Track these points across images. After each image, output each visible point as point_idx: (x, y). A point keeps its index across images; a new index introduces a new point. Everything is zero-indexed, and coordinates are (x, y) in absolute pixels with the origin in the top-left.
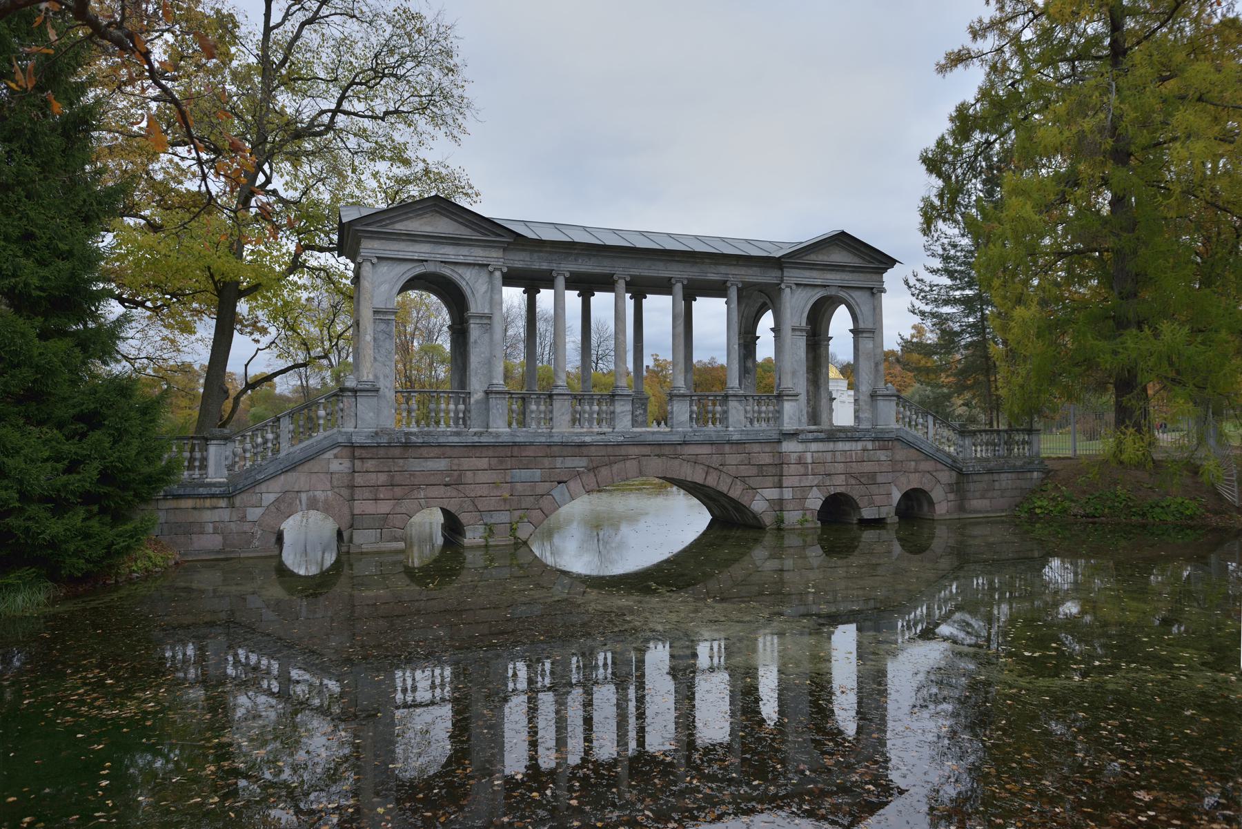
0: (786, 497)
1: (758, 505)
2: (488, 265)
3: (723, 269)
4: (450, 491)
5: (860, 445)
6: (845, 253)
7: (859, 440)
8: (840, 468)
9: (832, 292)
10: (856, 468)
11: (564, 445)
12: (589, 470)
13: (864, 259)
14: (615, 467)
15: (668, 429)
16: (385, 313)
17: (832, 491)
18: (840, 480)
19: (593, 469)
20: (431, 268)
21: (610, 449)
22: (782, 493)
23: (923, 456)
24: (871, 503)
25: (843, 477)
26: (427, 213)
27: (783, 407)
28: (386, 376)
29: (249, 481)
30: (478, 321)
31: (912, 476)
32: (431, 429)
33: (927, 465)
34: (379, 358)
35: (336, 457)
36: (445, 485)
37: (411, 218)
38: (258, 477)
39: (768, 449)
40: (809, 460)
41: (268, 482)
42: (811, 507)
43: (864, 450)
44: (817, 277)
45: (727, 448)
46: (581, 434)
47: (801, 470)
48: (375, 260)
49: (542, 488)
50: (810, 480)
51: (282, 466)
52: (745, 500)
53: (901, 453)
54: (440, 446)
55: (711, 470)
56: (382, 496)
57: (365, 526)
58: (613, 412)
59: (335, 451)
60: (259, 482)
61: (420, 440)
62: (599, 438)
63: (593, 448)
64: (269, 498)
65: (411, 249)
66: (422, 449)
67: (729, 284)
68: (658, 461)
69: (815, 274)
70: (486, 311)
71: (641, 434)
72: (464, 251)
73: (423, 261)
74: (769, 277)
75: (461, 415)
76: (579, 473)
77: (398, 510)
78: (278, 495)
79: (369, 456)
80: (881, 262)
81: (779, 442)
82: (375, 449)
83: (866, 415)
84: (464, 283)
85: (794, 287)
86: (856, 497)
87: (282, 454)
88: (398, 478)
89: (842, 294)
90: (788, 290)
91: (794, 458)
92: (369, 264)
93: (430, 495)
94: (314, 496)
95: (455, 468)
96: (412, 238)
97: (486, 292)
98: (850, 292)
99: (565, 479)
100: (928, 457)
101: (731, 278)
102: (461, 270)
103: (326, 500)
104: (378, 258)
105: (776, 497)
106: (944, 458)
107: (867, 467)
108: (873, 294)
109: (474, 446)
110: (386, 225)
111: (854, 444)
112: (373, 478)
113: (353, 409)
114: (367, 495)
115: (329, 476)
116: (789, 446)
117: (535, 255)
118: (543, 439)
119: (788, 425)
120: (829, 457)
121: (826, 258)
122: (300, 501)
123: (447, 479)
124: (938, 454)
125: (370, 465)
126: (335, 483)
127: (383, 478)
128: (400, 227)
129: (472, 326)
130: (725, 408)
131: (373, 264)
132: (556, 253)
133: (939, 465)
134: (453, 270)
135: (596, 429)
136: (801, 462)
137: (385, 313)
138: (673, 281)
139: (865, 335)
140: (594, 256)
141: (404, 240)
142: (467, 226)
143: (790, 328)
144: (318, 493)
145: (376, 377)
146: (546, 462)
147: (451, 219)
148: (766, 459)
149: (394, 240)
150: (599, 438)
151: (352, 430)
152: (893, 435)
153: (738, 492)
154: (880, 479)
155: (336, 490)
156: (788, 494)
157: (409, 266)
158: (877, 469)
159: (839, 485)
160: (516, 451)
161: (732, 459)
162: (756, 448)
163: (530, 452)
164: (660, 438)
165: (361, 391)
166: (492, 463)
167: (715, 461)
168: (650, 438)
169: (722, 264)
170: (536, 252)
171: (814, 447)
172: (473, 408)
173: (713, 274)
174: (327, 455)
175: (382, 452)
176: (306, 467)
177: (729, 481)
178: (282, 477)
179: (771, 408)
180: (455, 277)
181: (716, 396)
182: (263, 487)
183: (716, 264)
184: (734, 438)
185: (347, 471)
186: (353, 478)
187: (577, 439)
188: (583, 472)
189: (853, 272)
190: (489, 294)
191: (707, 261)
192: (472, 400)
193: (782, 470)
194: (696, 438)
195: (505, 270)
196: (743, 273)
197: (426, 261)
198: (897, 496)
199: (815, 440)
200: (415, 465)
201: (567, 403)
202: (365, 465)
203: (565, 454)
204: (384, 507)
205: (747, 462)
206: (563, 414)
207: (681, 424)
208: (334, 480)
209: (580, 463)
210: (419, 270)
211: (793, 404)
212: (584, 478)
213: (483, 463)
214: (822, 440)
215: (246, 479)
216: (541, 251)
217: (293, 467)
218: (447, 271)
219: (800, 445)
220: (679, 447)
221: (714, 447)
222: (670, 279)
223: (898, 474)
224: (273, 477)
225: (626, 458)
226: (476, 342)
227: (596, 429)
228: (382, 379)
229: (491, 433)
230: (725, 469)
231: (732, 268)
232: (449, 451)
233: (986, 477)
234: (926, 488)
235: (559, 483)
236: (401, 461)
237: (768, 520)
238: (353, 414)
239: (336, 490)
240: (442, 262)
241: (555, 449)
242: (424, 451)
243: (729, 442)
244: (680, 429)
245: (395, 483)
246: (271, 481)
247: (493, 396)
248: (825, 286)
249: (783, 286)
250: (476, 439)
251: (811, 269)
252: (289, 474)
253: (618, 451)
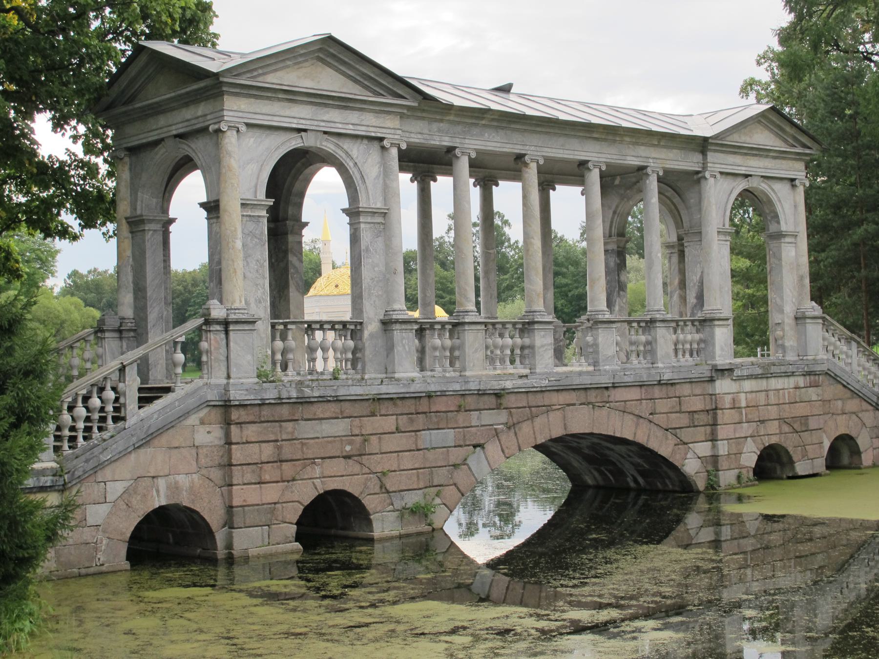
0: (721, 453)
1: (691, 467)
2: (381, 139)
3: (643, 151)
4: (353, 466)
5: (790, 382)
6: (767, 133)
7: (793, 374)
8: (773, 412)
9: (754, 183)
10: (789, 412)
11: (481, 393)
12: (509, 428)
13: (786, 141)
14: (538, 421)
15: (591, 368)
16: (254, 206)
18: (773, 427)
19: (510, 427)
20: (309, 141)
21: (530, 396)
22: (714, 447)
23: (849, 394)
24: (804, 455)
25: (776, 423)
26: (306, 61)
27: (712, 336)
28: (259, 301)
29: (92, 464)
30: (369, 219)
31: (842, 419)
32: (499, 372)
33: (853, 404)
34: (248, 274)
35: (202, 423)
36: (345, 457)
37: (288, 67)
38: (103, 458)
39: (698, 391)
40: (743, 404)
41: (114, 465)
42: (747, 464)
45: (657, 392)
46: (499, 377)
48: (243, 128)
49: (456, 455)
50: (746, 429)
51: (134, 439)
52: (676, 460)
53: (830, 390)
54: (337, 400)
55: (641, 420)
56: (267, 477)
57: (248, 523)
58: (531, 347)
59: (203, 413)
60: (100, 466)
61: (316, 394)
62: (520, 382)
63: (512, 398)
64: (116, 489)
65: (288, 112)
66: (315, 406)
67: (649, 170)
69: (738, 159)
70: (379, 205)
71: (568, 375)
72: (353, 117)
73: (299, 130)
74: (688, 162)
75: (279, 357)
76: (497, 433)
77: (288, 496)
78: (126, 484)
79: (251, 418)
80: (804, 146)
81: (712, 380)
82: (257, 409)
83: (791, 343)
84: (351, 164)
85: (718, 175)
86: (790, 449)
87: (131, 421)
88: (288, 451)
89: (764, 186)
90: (712, 180)
91: (728, 400)
92: (235, 133)
93: (327, 473)
94: (176, 483)
95: (357, 432)
96: (290, 96)
97: (377, 177)
98: (770, 182)
99: (482, 442)
100: (855, 394)
101: (651, 163)
102: (347, 144)
103: (191, 488)
104: (248, 125)
105: (708, 453)
106: (869, 394)
107: (800, 410)
108: (794, 186)
109: (378, 400)
110: (260, 75)
111: (786, 380)
112: (254, 452)
113: (223, 350)
114: (249, 477)
115: (194, 451)
116: (723, 386)
117: (435, 126)
118: (457, 387)
121: (748, 140)
122: (158, 491)
123: (348, 448)
124: (864, 391)
125: (251, 432)
126: (203, 461)
127: (268, 451)
128: (273, 79)
129: (362, 226)
130: (650, 338)
131: (238, 131)
132: (459, 123)
133: (864, 404)
134: (337, 145)
135: (510, 370)
137: (254, 206)
138: (590, 165)
139: (787, 240)
140: (503, 128)
141: (279, 100)
142: (356, 81)
143: (716, 230)
144: (181, 479)
145: (247, 303)
146: (461, 418)
147: (338, 70)
148: (697, 404)
149: (268, 98)
150: (520, 382)
151: (225, 381)
152: (824, 368)
153: (670, 449)
154: (813, 423)
155: (204, 472)
156: (723, 448)
157: (283, 137)
159: (772, 435)
160: (424, 406)
161: (663, 406)
162: (686, 390)
163: (440, 405)
164: (587, 380)
165: (237, 322)
166: (400, 422)
167: (644, 408)
168: (577, 381)
169: (643, 144)
170: (436, 120)
171: (748, 385)
172: (367, 345)
173: (632, 157)
174: (193, 420)
175: (266, 412)
176: (164, 440)
177: (660, 433)
178: (133, 455)
179: (697, 337)
180: (340, 155)
181: (639, 322)
182: (107, 473)
183: (636, 144)
184: (666, 377)
185: (217, 442)
186: (230, 452)
187: (496, 385)
188: (503, 431)
189: (775, 158)
190: (381, 181)
191: (627, 139)
192: (366, 334)
193: (715, 418)
194: (626, 379)
195: (404, 146)
196: (663, 156)
197: (305, 130)
198: (827, 444)
199: (750, 377)
200: (307, 430)
201: (481, 335)
202: (245, 433)
203: (481, 406)
204: (271, 493)
205: (678, 409)
206: (476, 351)
208: (200, 456)
209: (499, 418)
210: (294, 142)
211: (724, 330)
212: (503, 438)
213: (389, 423)
214: (756, 377)
215: (87, 461)
216: (441, 121)
217: (147, 440)
218: (328, 146)
219: (733, 383)
220: (606, 393)
221: (643, 389)
222: (587, 162)
223: (827, 417)
224: (125, 454)
225: (549, 408)
226: (367, 250)
227: (510, 370)
228: (253, 305)
229: (398, 380)
230: (656, 418)
231: (652, 149)
232: (348, 408)
234: (853, 434)
235: (475, 446)
236: (289, 426)
237: (701, 485)
238: (223, 358)
239: (204, 472)
240: (325, 133)
241: (469, 399)
242: (319, 410)
243: (660, 383)
244: (607, 367)
245: (284, 457)
246: (118, 463)
247: (398, 326)
248: (747, 176)
249: (707, 175)
250: (384, 389)
251: (735, 153)
252: (142, 451)
253: (538, 400)
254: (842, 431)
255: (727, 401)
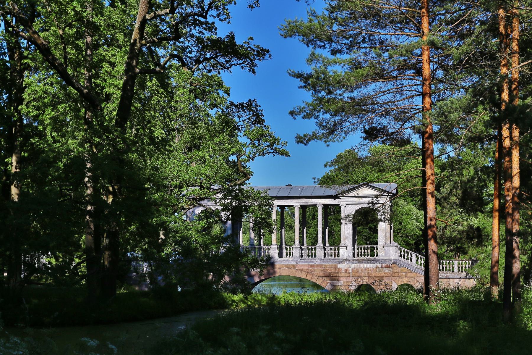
5: (375, 266)
10: (373, 274)
17: (361, 283)
31: (404, 279)
33: (413, 275)
40: (351, 271)
43: (377, 268)
44: (356, 201)
47: (348, 275)
53: (397, 270)
68: (287, 269)
85: (345, 205)
91: (343, 270)
107: (379, 275)
119: (341, 257)
120: (360, 270)
136: (346, 271)
158: (383, 275)
162: (328, 266)
164: (287, 262)
168: (283, 262)
184: (318, 262)
207: (296, 257)
214: (356, 263)
223: (397, 278)
233: (446, 280)
254: (405, 282)
255: (343, 270)
